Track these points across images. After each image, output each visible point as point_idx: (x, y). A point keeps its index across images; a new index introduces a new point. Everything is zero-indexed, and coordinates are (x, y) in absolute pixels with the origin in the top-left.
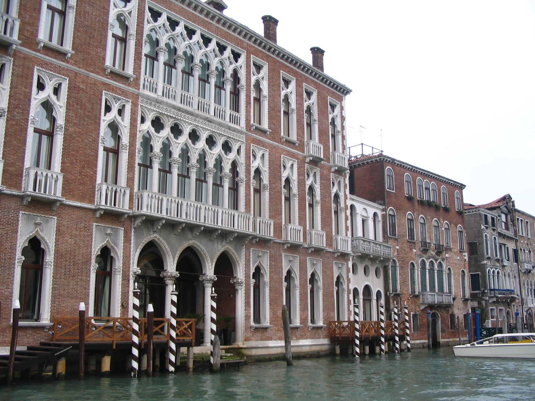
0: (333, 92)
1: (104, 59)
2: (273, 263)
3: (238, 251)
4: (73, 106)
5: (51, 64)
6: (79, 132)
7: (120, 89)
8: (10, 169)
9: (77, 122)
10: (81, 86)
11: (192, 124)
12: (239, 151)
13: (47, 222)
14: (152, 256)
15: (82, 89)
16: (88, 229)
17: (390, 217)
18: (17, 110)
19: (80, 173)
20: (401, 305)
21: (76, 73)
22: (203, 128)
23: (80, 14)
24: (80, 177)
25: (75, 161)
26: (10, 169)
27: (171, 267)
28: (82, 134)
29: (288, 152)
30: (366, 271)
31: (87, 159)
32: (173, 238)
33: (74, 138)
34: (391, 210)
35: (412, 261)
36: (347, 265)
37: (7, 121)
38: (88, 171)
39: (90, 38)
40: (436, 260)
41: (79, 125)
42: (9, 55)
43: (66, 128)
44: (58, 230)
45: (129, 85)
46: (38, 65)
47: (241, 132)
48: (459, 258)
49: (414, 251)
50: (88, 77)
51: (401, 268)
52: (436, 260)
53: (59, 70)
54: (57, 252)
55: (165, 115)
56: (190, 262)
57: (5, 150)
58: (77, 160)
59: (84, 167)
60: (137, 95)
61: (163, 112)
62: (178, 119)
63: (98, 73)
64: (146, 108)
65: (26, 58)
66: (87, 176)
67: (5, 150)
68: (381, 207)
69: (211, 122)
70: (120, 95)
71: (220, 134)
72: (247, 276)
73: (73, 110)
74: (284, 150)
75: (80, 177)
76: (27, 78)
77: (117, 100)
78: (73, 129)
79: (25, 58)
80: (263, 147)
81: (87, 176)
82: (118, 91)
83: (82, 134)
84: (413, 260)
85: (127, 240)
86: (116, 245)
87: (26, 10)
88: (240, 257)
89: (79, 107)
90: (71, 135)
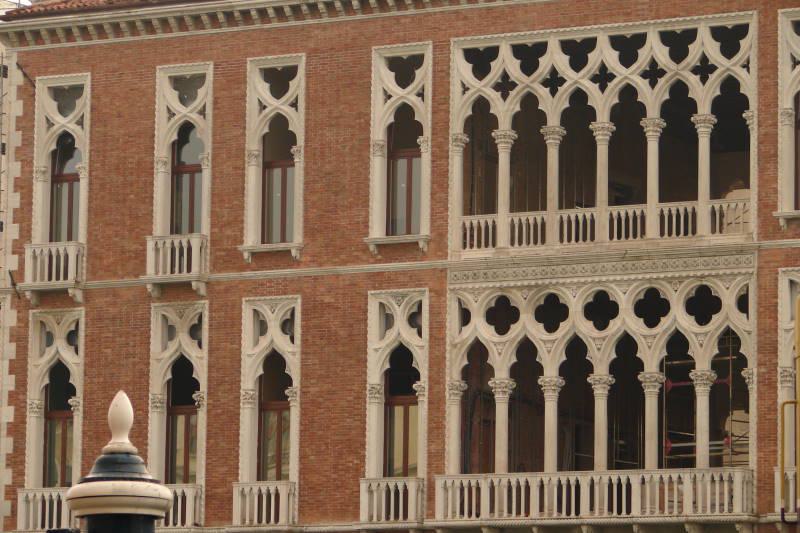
1: (367, 226)
4: (314, 344)
5: (270, 281)
6: (330, 392)
7: (404, 273)
8: (219, 491)
9: (323, 372)
10: (327, 299)
11: (585, 283)
12: (743, 304)
15: (329, 305)
18: (222, 388)
19: (335, 467)
21: (316, 278)
22: (615, 281)
23: (314, 155)
24: (334, 476)
25: (323, 448)
26: (219, 491)
28: (334, 393)
31: (347, 437)
33: (320, 403)
37: (209, 411)
38: (350, 459)
39: (336, 194)
41: (328, 377)
42: (202, 297)
43: (304, 390)
45: (424, 256)
46: (250, 292)
47: (741, 250)
50: (337, 276)
53: (284, 287)
55: (512, 287)
57: (209, 461)
58: (326, 444)
59: (340, 455)
60: (442, 271)
61: (505, 284)
62: (547, 286)
63: (356, 260)
64: (465, 290)
65: (229, 288)
66: (347, 470)
67: (209, 461)
69: (638, 258)
70: (404, 285)
71: (670, 280)
73: (315, 353)
75: (334, 476)
76: (233, 325)
77: (399, 298)
78: (317, 389)
79: (227, 290)
81: (347, 470)
82: (402, 279)
83: (334, 393)
87: (222, 201)
89: (324, 342)
90: (313, 402)
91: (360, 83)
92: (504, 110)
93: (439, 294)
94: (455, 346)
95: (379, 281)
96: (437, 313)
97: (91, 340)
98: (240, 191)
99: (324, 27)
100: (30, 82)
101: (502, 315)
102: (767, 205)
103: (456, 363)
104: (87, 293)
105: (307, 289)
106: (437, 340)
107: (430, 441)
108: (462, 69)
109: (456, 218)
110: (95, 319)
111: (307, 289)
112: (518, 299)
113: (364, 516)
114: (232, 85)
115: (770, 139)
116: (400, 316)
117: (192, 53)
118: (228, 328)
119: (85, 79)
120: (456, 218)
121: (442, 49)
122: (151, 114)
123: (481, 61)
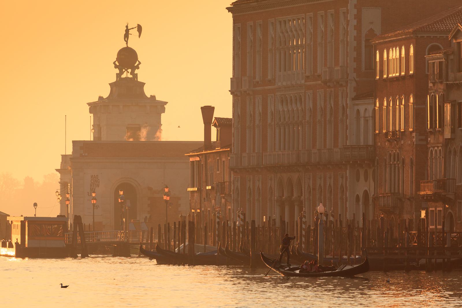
36: (346, 174)
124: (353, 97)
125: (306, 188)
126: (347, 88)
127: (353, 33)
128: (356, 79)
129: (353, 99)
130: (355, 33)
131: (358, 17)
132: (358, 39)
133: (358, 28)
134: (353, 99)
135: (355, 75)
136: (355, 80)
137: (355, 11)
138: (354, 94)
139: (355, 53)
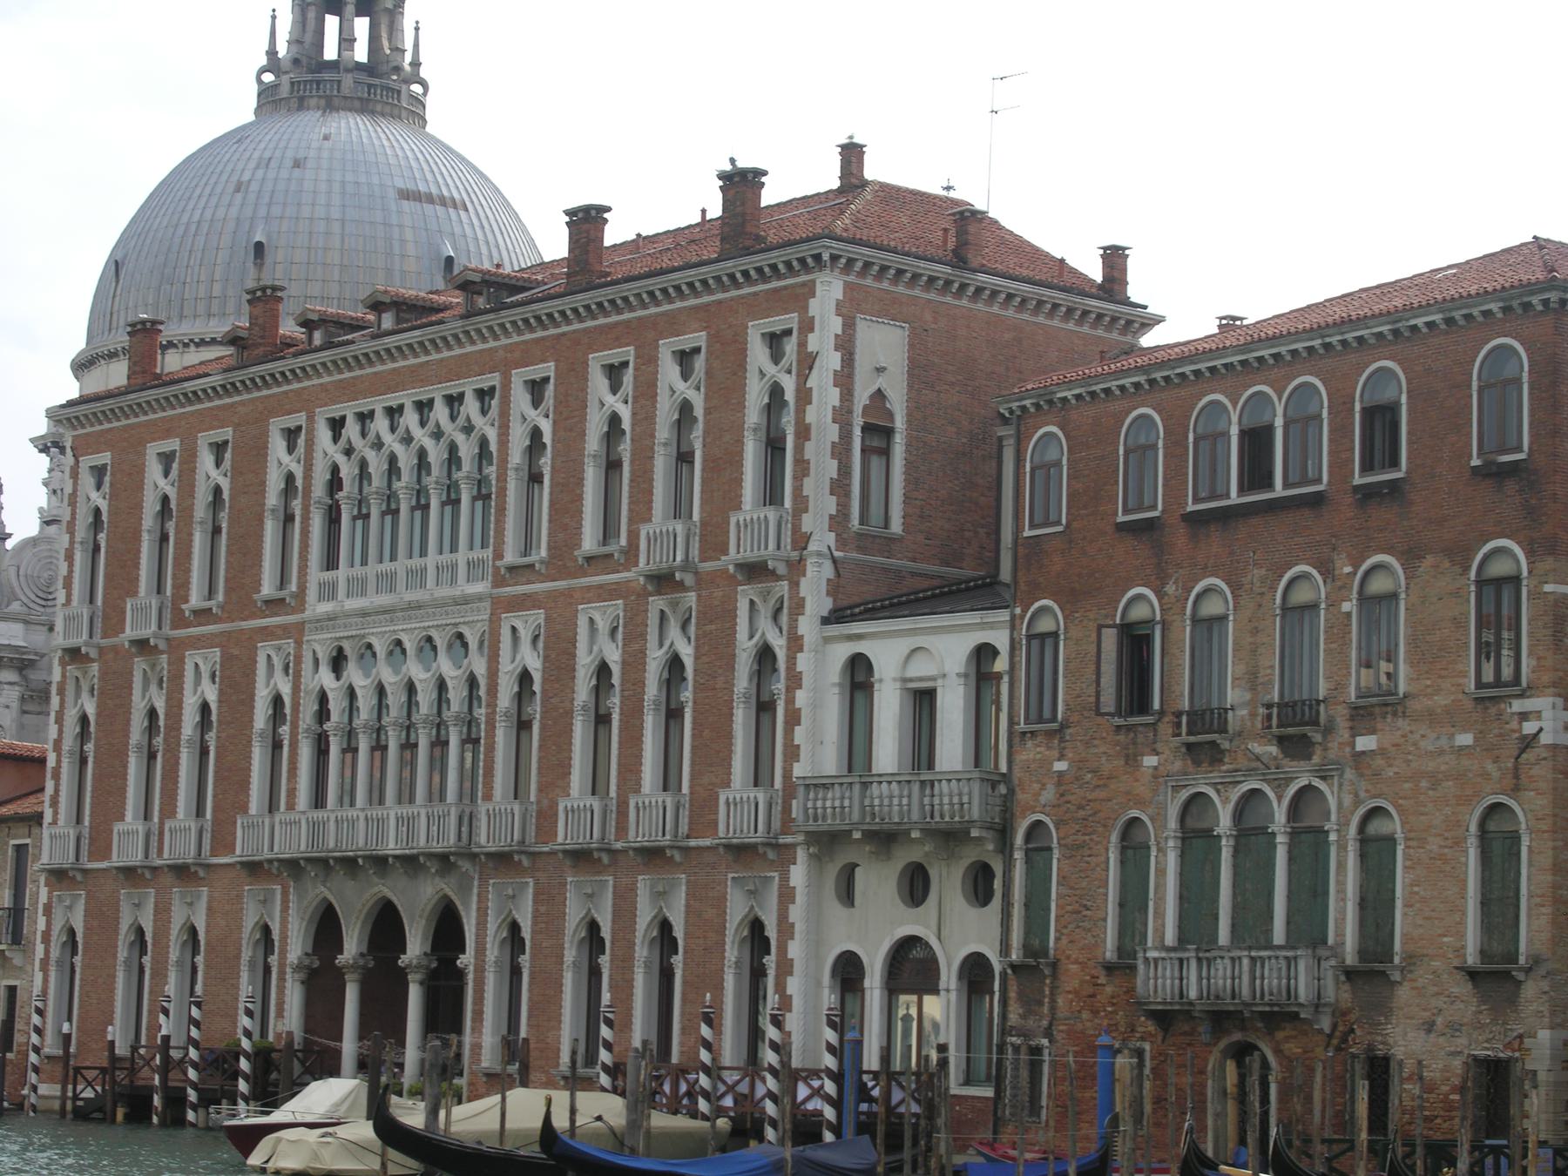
0: (775, 290)
2: (543, 909)
3: (465, 889)
10: (236, 652)
13: (199, 897)
14: (327, 928)
16: (240, 897)
17: (1035, 643)
20: (1053, 1008)
27: (352, 946)
29: (600, 586)
30: (916, 886)
32: (349, 886)
34: (1050, 614)
35: (1135, 813)
36: (785, 878)
40: (1280, 785)
44: (209, 909)
45: (294, 611)
48: (1465, 739)
49: (1150, 761)
51: (1072, 850)
52: (1280, 785)
54: (207, 944)
56: (386, 927)
68: (1004, 616)
69: (420, 607)
72: (480, 950)
74: (589, 588)
80: (534, 607)
84: (1141, 803)
85: (285, 909)
86: (272, 919)
88: (467, 905)
91: (257, 452)
92: (348, 471)
93: (299, 643)
94: (306, 693)
95: (267, 633)
96: (298, 659)
97: (101, 693)
98: (189, 555)
99: (242, 403)
100: (77, 462)
101: (338, 662)
102: (498, 555)
103: (309, 708)
104: (102, 650)
105: (222, 641)
106: (296, 689)
107: (289, 780)
108: (324, 435)
109: (316, 575)
110: (104, 675)
111: (222, 641)
112: (346, 645)
113: (238, 851)
114: (190, 456)
115: (502, 491)
116: (278, 663)
117: (168, 434)
118: (177, 678)
119: (105, 458)
120: (316, 575)
121: (311, 419)
122: (140, 487)
123: (337, 425)
124: (825, 614)
125: (492, 927)
126: (795, 585)
127: (826, 395)
128: (837, 554)
129: (826, 621)
130: (834, 396)
131: (846, 345)
132: (842, 416)
133: (845, 380)
134: (826, 621)
135: (831, 538)
136: (834, 561)
137: (836, 325)
138: (827, 605)
139: (835, 463)
